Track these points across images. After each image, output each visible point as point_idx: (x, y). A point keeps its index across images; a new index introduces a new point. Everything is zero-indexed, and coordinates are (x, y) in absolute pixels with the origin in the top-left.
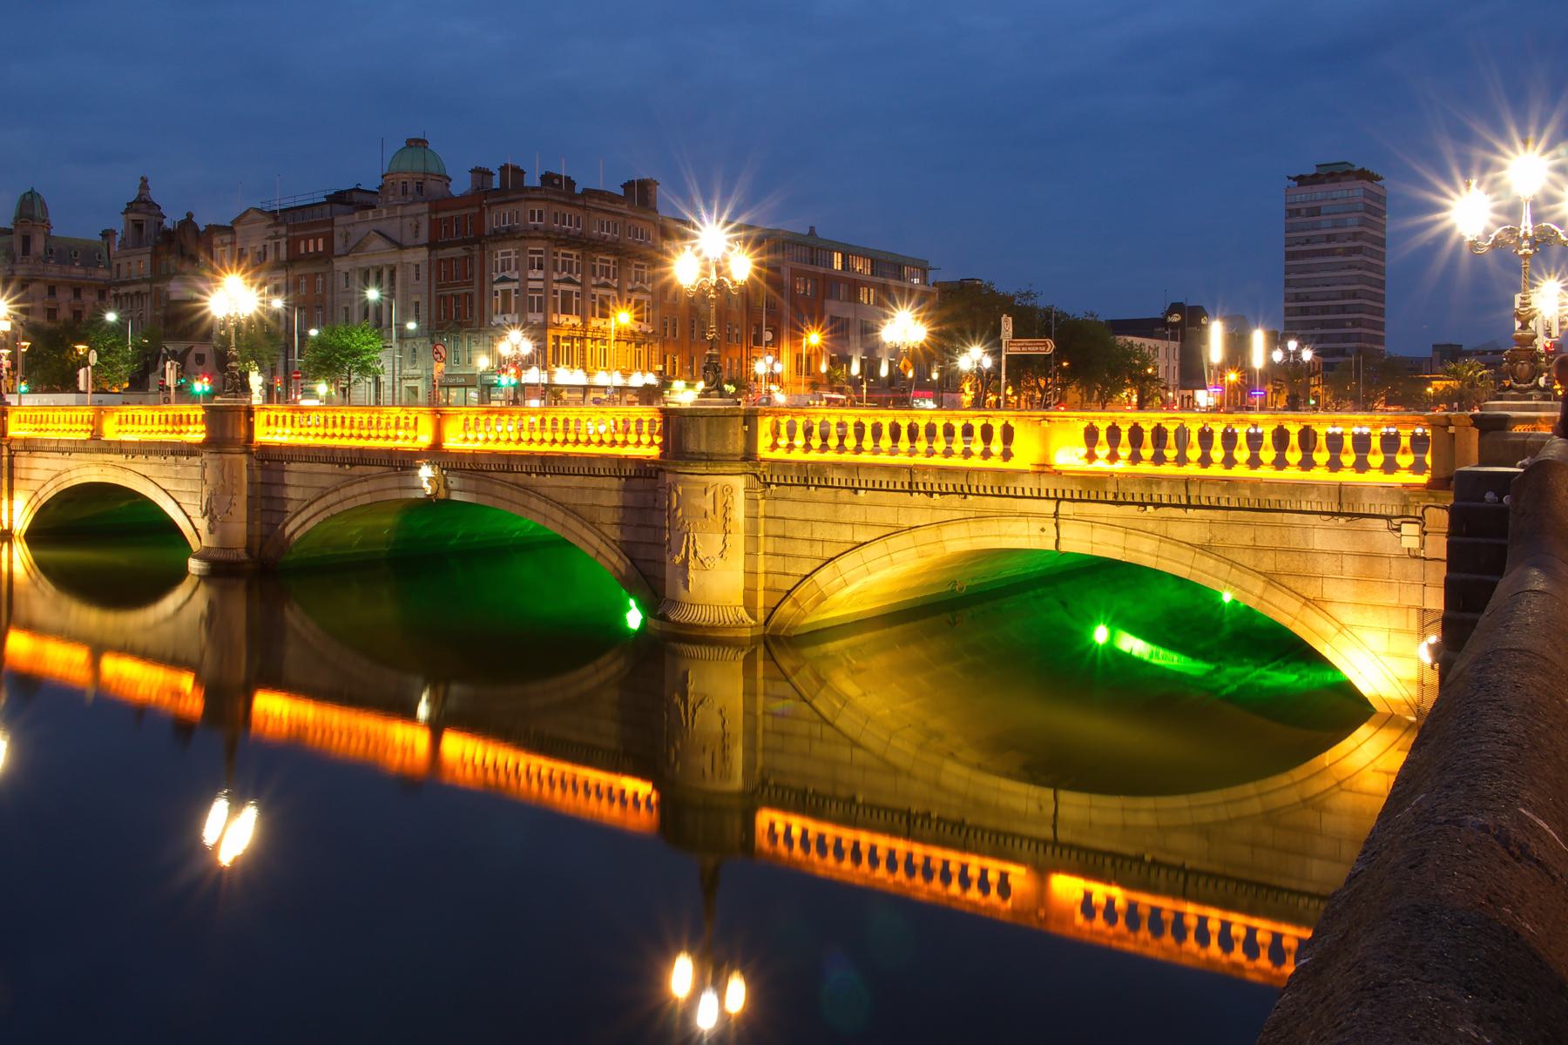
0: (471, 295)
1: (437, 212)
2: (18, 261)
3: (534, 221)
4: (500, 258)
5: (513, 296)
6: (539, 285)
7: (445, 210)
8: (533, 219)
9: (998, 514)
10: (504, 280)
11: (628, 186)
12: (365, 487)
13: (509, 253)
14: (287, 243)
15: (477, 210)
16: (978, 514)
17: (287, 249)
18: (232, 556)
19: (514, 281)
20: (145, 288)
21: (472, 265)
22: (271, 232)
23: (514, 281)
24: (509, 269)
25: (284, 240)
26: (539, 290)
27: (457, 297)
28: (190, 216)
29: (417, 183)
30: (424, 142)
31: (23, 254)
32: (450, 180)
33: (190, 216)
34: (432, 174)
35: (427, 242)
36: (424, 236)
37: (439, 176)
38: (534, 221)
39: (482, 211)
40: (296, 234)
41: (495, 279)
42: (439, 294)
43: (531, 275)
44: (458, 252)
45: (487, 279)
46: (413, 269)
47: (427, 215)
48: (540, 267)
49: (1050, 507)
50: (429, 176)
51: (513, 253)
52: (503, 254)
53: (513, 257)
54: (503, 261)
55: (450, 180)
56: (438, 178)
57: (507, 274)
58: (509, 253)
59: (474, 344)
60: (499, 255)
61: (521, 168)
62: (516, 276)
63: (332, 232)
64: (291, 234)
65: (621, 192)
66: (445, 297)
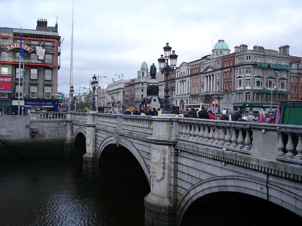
0: (231, 81)
1: (223, 59)
2: (141, 78)
3: (248, 60)
4: (239, 70)
5: (242, 81)
7: (225, 59)
8: (247, 59)
9: (245, 176)
10: (239, 77)
14: (191, 70)
15: (233, 58)
16: (238, 175)
17: (191, 72)
20: (163, 83)
21: (232, 73)
22: (187, 68)
24: (241, 74)
25: (190, 70)
26: (249, 80)
27: (228, 82)
28: (154, 64)
29: (220, 52)
30: (224, 41)
31: (142, 77)
32: (230, 51)
33: (154, 64)
34: (224, 49)
37: (227, 49)
38: (248, 60)
40: (193, 68)
42: (224, 82)
43: (247, 75)
44: (228, 70)
47: (221, 61)
48: (250, 73)
49: (264, 177)
50: (224, 50)
51: (242, 69)
53: (242, 70)
55: (230, 51)
56: (226, 50)
58: (241, 69)
59: (232, 95)
60: (239, 70)
61: (247, 45)
62: (243, 76)
63: (200, 67)
64: (191, 68)
66: (225, 82)
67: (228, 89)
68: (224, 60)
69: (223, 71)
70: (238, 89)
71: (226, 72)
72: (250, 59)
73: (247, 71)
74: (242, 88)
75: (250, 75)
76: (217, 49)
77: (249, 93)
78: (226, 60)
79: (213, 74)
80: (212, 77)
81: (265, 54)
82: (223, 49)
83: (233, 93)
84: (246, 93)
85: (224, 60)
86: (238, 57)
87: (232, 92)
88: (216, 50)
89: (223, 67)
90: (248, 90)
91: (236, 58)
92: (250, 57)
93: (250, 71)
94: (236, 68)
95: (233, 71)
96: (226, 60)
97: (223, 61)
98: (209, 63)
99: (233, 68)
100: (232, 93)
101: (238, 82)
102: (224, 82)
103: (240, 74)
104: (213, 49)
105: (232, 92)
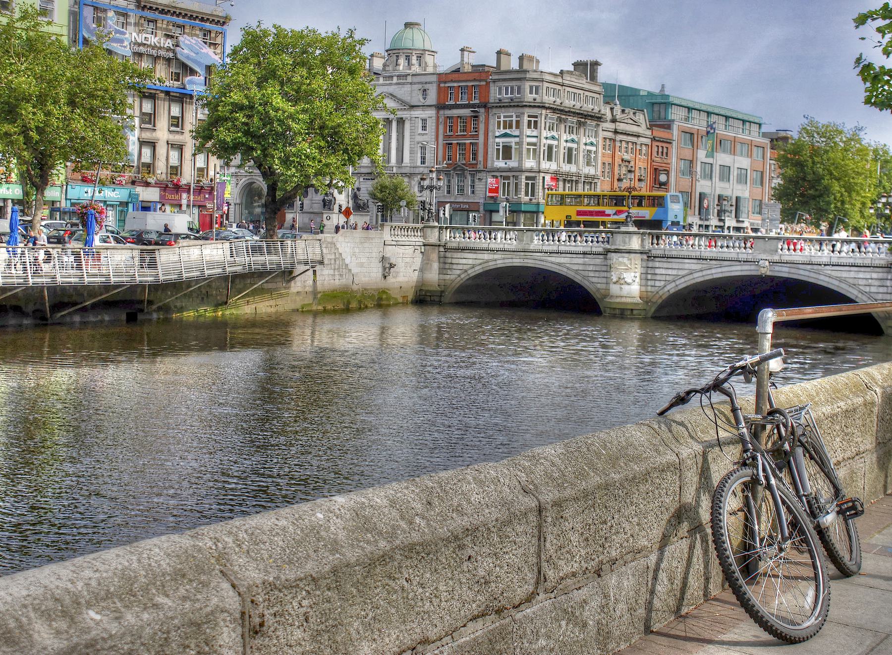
0: (476, 144)
1: (445, 83)
4: (502, 119)
6: (534, 140)
7: (452, 81)
10: (505, 135)
11: (576, 65)
12: (719, 270)
13: (512, 117)
15: (483, 83)
18: (635, 301)
19: (515, 136)
23: (515, 136)
26: (535, 144)
35: (434, 103)
36: (432, 98)
39: (488, 84)
41: (497, 134)
42: (445, 142)
44: (466, 112)
45: (490, 134)
46: (420, 122)
50: (427, 52)
51: (514, 116)
52: (505, 117)
53: (514, 119)
54: (505, 122)
57: (508, 131)
58: (512, 117)
60: (502, 117)
65: (572, 68)
67: (464, 162)
68: (447, 85)
69: (441, 112)
70: (500, 164)
71: (455, 119)
72: (537, 93)
73: (529, 122)
74: (512, 164)
75: (535, 133)
76: (410, 49)
77: (533, 178)
78: (455, 85)
79: (404, 116)
80: (394, 124)
81: (564, 81)
82: (425, 50)
83: (480, 174)
84: (527, 178)
85: (447, 85)
86: (500, 84)
87: (480, 171)
88: (405, 51)
89: (442, 102)
90: (530, 171)
91: (491, 85)
92: (537, 88)
93: (536, 122)
94: (495, 111)
95: (482, 118)
96: (455, 85)
97: (442, 85)
98: (383, 85)
99: (482, 110)
100: (479, 175)
101: (501, 147)
102: (445, 142)
103: (505, 128)
104: (388, 47)
105: (480, 171)
